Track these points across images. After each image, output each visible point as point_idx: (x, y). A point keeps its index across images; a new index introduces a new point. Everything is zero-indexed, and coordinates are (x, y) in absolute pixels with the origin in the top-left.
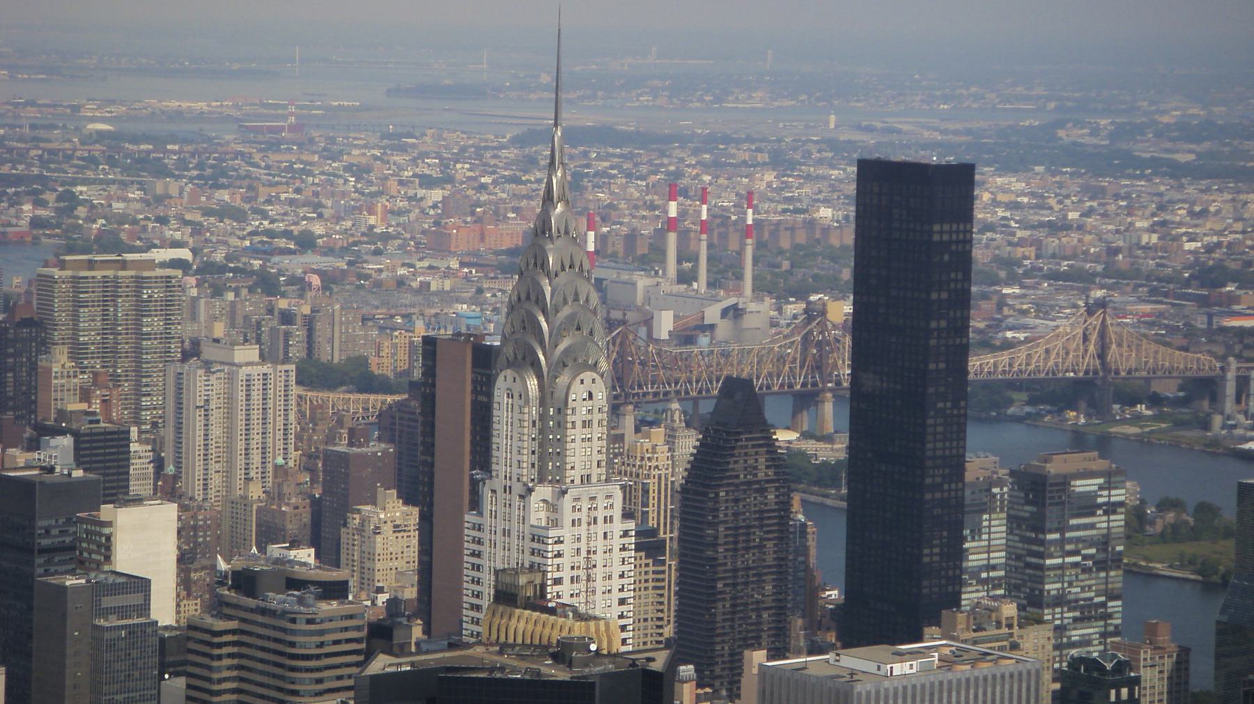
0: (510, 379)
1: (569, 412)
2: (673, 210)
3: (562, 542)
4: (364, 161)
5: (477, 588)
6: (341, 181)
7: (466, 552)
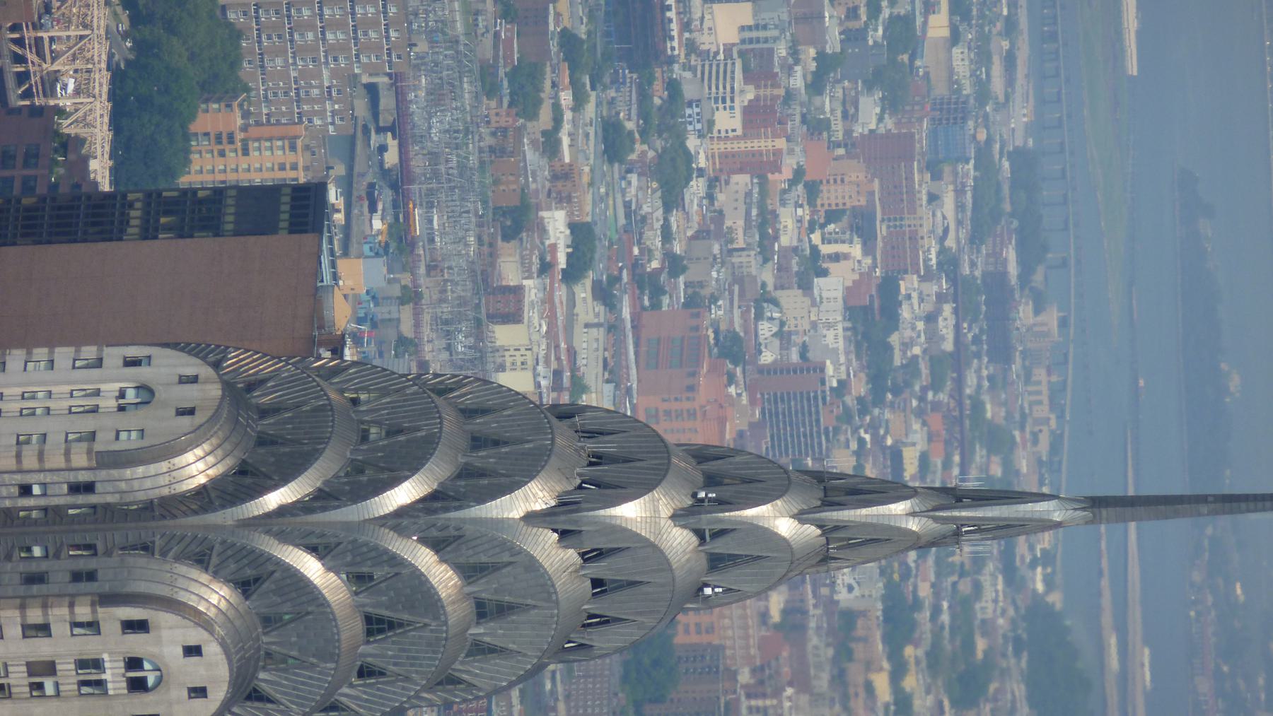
0: (190, 395)
1: (83, 612)
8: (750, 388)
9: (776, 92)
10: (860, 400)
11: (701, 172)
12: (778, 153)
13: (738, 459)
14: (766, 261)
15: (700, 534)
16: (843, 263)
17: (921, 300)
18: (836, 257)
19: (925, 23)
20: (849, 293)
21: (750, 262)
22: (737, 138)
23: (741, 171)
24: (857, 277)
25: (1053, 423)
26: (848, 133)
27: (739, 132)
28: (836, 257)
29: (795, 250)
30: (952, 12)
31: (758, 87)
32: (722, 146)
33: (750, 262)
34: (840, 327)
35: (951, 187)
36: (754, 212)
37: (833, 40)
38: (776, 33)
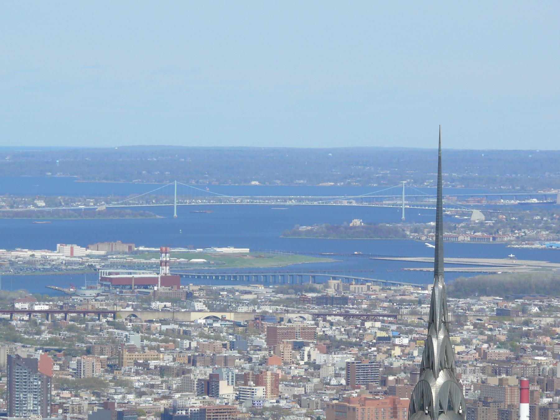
8: (354, 388)
9: (251, 374)
10: (360, 350)
11: (278, 402)
12: (272, 374)
13: (414, 398)
14: (309, 381)
15: (441, 413)
16: (311, 353)
17: (325, 327)
18: (309, 356)
19: (229, 321)
20: (322, 352)
21: (310, 386)
22: (266, 389)
23: (278, 387)
24: (316, 349)
25: (369, 284)
26: (266, 349)
27: (264, 387)
28: (309, 356)
29: (306, 370)
30: (226, 312)
31: (249, 380)
32: (269, 394)
33: (310, 386)
34: (334, 356)
35: (286, 315)
36: (292, 384)
37: (235, 353)
38: (230, 373)
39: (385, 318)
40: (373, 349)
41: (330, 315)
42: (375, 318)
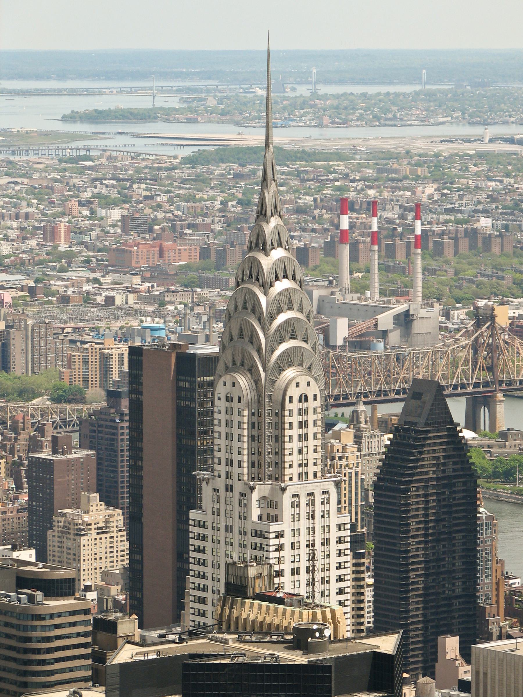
2: (345, 222)
3: (282, 536)
4: (44, 183)
5: (202, 582)
6: (24, 203)
7: (191, 548)
39: (148, 181)
40: (141, 205)
41: (105, 179)
42: (140, 181)
